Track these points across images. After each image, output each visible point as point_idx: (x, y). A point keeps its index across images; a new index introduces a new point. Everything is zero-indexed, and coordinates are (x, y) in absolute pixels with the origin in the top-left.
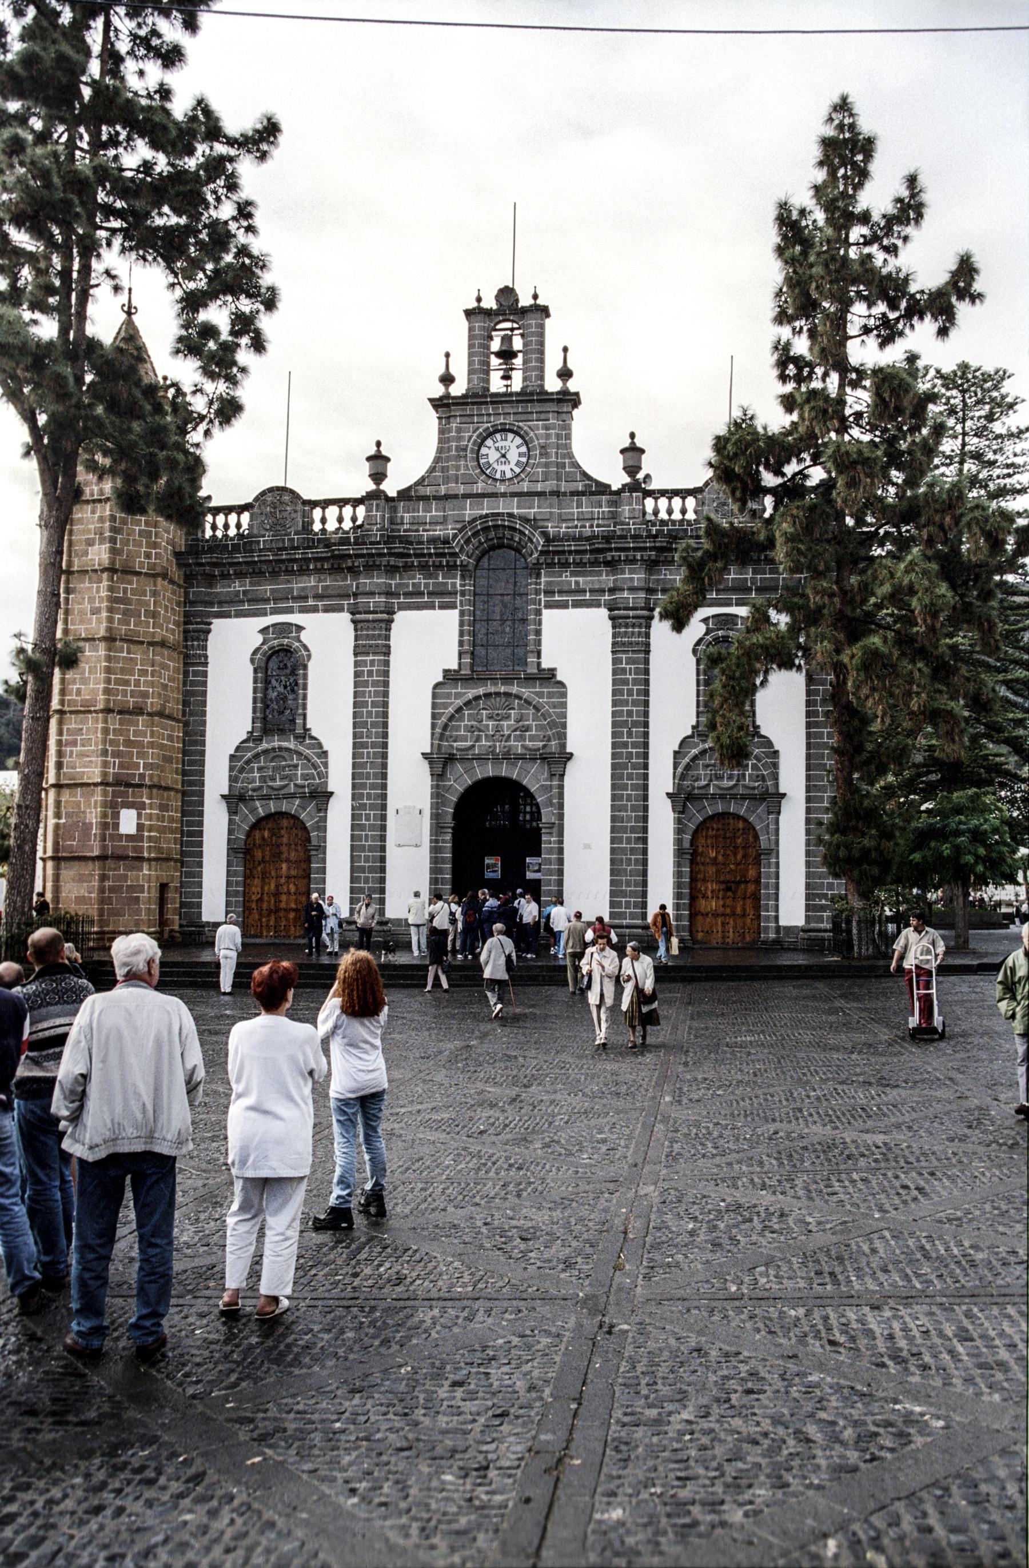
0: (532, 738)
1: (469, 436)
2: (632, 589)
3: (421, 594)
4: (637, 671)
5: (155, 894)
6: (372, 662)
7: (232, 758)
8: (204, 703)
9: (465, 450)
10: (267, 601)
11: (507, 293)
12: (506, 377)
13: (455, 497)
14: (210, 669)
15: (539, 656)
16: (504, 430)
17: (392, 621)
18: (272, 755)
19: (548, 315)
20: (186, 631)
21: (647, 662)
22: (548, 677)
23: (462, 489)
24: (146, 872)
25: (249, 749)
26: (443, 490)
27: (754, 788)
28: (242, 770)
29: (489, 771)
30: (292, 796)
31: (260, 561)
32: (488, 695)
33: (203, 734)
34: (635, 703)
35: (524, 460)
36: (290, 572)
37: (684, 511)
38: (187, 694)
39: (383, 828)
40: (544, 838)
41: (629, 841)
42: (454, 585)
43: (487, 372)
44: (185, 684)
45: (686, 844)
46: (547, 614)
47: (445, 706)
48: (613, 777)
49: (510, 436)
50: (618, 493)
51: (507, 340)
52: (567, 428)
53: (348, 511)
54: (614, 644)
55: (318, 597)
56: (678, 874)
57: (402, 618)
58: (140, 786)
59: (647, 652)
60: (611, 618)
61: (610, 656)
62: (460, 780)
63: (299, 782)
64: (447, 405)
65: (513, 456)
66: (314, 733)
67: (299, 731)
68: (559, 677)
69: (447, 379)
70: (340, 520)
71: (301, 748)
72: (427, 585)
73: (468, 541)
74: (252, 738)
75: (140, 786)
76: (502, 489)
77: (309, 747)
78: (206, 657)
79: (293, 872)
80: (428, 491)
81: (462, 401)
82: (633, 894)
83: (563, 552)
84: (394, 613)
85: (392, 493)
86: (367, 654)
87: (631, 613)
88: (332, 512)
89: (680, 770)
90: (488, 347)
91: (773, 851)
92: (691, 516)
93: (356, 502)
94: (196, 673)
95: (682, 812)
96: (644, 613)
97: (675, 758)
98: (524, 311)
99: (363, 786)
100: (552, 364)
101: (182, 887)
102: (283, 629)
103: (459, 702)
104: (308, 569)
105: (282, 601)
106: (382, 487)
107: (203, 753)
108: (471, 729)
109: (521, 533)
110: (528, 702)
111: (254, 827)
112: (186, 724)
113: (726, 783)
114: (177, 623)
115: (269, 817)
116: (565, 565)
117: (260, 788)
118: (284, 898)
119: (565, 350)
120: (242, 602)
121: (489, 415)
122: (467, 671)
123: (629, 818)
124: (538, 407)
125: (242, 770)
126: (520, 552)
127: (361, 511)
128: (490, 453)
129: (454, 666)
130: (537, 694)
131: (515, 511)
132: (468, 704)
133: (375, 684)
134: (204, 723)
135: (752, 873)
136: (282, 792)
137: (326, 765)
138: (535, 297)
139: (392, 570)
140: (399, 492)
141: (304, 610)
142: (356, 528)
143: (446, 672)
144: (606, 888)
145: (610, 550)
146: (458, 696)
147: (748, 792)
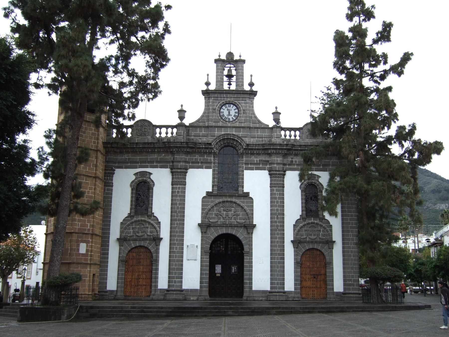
0: (240, 219)
1: (217, 105)
2: (278, 164)
4: (280, 194)
6: (179, 188)
7: (122, 223)
9: (215, 110)
10: (138, 162)
11: (230, 54)
12: (230, 84)
13: (212, 127)
14: (114, 188)
15: (243, 188)
16: (230, 103)
17: (187, 172)
18: (311, 225)
19: (245, 63)
20: (105, 173)
21: (283, 191)
22: (247, 195)
23: (214, 124)
24: (89, 269)
25: (129, 220)
27: (323, 239)
28: (125, 228)
29: (224, 231)
30: (146, 239)
31: (136, 147)
32: (224, 202)
35: (237, 114)
36: (148, 152)
37: (295, 136)
38: (104, 197)
39: (182, 253)
40: (245, 257)
41: (278, 259)
43: (223, 82)
44: (104, 194)
45: (299, 260)
47: (207, 205)
49: (232, 106)
50: (272, 128)
51: (230, 71)
53: (170, 130)
54: (271, 184)
55: (157, 162)
59: (284, 187)
61: (269, 188)
62: (213, 234)
63: (149, 234)
66: (155, 215)
67: (149, 214)
69: (208, 84)
70: (167, 133)
71: (150, 221)
72: (200, 159)
73: (217, 143)
74: (130, 216)
77: (153, 220)
78: (112, 183)
79: (145, 270)
80: (201, 124)
81: (214, 92)
83: (252, 149)
84: (187, 169)
86: (177, 185)
87: (278, 173)
88: (164, 130)
91: (331, 263)
92: (298, 138)
93: (172, 127)
94: (108, 190)
95: (297, 248)
96: (282, 172)
97: (294, 227)
98: (237, 61)
99: (175, 236)
100: (246, 81)
101: (100, 276)
103: (213, 204)
104: (155, 151)
105: (144, 163)
106: (184, 121)
107: (110, 221)
108: (216, 215)
110: (239, 205)
111: (129, 251)
113: (313, 237)
114: (102, 170)
115: (136, 247)
116: (253, 154)
117: (132, 236)
118: (141, 280)
119: (251, 76)
122: (215, 192)
123: (278, 250)
124: (242, 96)
125: (125, 228)
127: (175, 130)
128: (225, 111)
129: (210, 190)
131: (234, 133)
132: (216, 205)
135: (323, 272)
139: (187, 153)
140: (190, 124)
142: (172, 136)
144: (269, 277)
146: (212, 202)
147: (321, 240)
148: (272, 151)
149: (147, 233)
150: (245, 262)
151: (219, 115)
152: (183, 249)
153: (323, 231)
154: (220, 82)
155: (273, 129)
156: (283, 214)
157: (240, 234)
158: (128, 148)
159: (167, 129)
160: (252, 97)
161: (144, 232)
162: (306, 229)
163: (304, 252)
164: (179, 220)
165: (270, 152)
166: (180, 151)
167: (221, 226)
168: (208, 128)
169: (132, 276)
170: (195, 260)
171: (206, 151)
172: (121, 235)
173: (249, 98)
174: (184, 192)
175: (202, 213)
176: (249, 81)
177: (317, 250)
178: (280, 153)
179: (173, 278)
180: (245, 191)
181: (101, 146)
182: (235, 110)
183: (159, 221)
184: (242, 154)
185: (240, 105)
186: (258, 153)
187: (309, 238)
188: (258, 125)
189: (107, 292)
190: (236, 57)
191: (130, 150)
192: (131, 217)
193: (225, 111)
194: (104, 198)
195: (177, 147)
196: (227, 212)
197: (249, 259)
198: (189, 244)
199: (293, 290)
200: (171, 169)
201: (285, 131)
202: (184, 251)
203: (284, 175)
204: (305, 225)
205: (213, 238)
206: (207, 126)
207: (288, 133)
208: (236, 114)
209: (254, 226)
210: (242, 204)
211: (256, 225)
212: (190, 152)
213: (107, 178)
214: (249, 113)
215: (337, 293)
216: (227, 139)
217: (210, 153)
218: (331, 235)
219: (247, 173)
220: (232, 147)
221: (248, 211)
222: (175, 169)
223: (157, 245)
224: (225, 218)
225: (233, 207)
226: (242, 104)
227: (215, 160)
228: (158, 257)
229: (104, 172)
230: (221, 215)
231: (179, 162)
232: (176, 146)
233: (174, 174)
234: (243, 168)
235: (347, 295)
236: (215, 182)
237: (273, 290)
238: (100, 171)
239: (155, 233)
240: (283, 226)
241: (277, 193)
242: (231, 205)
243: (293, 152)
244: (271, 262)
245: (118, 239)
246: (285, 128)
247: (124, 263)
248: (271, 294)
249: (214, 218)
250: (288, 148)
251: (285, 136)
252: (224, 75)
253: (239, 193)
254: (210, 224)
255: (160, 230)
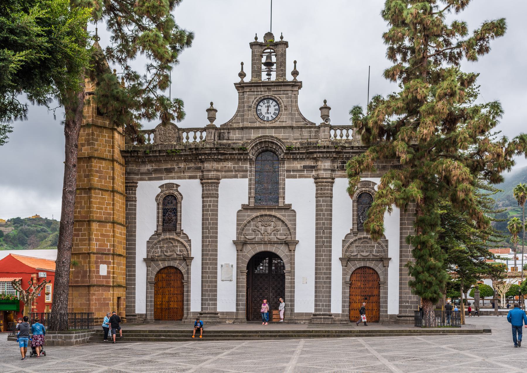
0: (281, 235)
1: (253, 100)
2: (325, 170)
3: (232, 171)
5: (116, 301)
7: (148, 242)
8: (135, 218)
11: (269, 35)
12: (269, 75)
13: (247, 128)
14: (137, 203)
15: (284, 199)
16: (268, 99)
17: (219, 183)
19: (287, 47)
20: (126, 186)
21: (331, 201)
22: (288, 208)
23: (249, 125)
25: (155, 239)
26: (241, 125)
27: (377, 256)
30: (175, 259)
32: (261, 216)
33: (135, 232)
34: (326, 219)
35: (277, 112)
37: (347, 136)
38: (127, 214)
39: (216, 273)
40: (286, 277)
41: (323, 278)
42: (246, 167)
44: (126, 210)
45: (348, 280)
46: (287, 181)
47: (243, 220)
48: (316, 251)
49: (271, 101)
50: (319, 127)
51: (269, 57)
52: (296, 98)
53: (198, 134)
56: (344, 293)
57: (223, 181)
58: (108, 254)
59: (332, 197)
60: (316, 183)
61: (315, 199)
62: (250, 252)
63: (178, 253)
64: (243, 87)
65: (272, 110)
66: (184, 232)
68: (293, 208)
70: (195, 138)
71: (179, 239)
72: (234, 167)
73: (253, 148)
74: (157, 234)
75: (108, 254)
76: (268, 125)
77: (182, 238)
78: (136, 198)
79: (176, 292)
80: (235, 125)
81: (251, 85)
82: (325, 301)
83: (295, 153)
85: (218, 126)
86: (208, 197)
88: (191, 134)
89: (345, 248)
90: (261, 61)
91: (386, 283)
94: (131, 205)
95: (346, 266)
96: (330, 180)
97: (343, 243)
98: (277, 44)
99: (207, 255)
100: (289, 68)
101: (126, 299)
102: (169, 186)
103: (249, 219)
107: (135, 240)
108: (254, 231)
109: (276, 144)
110: (279, 219)
111: (158, 272)
112: (127, 227)
113: (365, 254)
115: (165, 268)
116: (295, 159)
117: (161, 256)
118: (172, 303)
120: (151, 174)
121: (261, 91)
122: (252, 205)
124: (283, 88)
125: (153, 248)
126: (275, 154)
127: (204, 134)
128: (263, 108)
130: (283, 215)
131: (273, 135)
132: (253, 219)
133: (212, 210)
134: (135, 227)
135: (375, 292)
136: (170, 257)
137: (190, 246)
138: (282, 38)
139: (219, 161)
140: (221, 126)
141: (179, 178)
143: (243, 205)
145: (316, 152)
146: (249, 216)
148: (318, 155)
149: (176, 251)
150: (286, 283)
151: (255, 113)
152: (216, 269)
153: (377, 247)
154: (256, 72)
155: (320, 128)
156: (331, 229)
157: (281, 251)
158: (150, 156)
159: (195, 132)
160: (295, 90)
161: (173, 251)
162: (357, 245)
163: (354, 271)
164: (211, 237)
165: (315, 156)
166: (209, 159)
167: (259, 243)
168: (243, 129)
169: (162, 299)
170: (231, 281)
171: (240, 157)
172: (147, 255)
173: (292, 91)
174: (217, 206)
175: (237, 229)
176: (292, 69)
177: (370, 268)
178: (328, 157)
179: (207, 300)
180: (287, 202)
181: (117, 155)
182: (274, 106)
183: (190, 239)
184: (283, 160)
185: (281, 100)
186: (301, 158)
187: (361, 255)
188: (302, 124)
189: (135, 316)
190: (277, 39)
191: (153, 159)
192: (157, 235)
193: (263, 108)
194: (126, 215)
195: (205, 154)
196: (265, 227)
197: (291, 279)
198: (223, 264)
199: (340, 312)
200: (201, 180)
201: (335, 130)
202: (218, 271)
203: (333, 183)
204: (355, 241)
205: (250, 256)
206: (242, 127)
207: (338, 132)
208: (276, 112)
209: (297, 242)
210: (282, 218)
211: (298, 241)
212: (222, 159)
213: (129, 193)
214: (292, 109)
215: (390, 315)
216: (265, 142)
217: (245, 160)
218: (386, 251)
219: (289, 182)
220: (271, 151)
221: (289, 226)
222: (205, 179)
223: (188, 265)
224: (263, 234)
225: (273, 222)
226: (284, 100)
227: (251, 168)
228: (189, 278)
229: (124, 185)
230: (258, 231)
231: (209, 171)
232: (204, 152)
233: (204, 185)
234: (284, 176)
235: (402, 318)
236: (252, 193)
237: (318, 313)
238: (118, 184)
239: (185, 252)
240: (330, 242)
241: (324, 204)
242: (270, 219)
243: (343, 156)
244: (315, 281)
245: (145, 260)
246: (335, 126)
247: (153, 285)
248: (315, 317)
249: (251, 235)
250: (337, 150)
251: (335, 136)
252: (262, 63)
253: (279, 205)
254: (247, 241)
255: (191, 249)
